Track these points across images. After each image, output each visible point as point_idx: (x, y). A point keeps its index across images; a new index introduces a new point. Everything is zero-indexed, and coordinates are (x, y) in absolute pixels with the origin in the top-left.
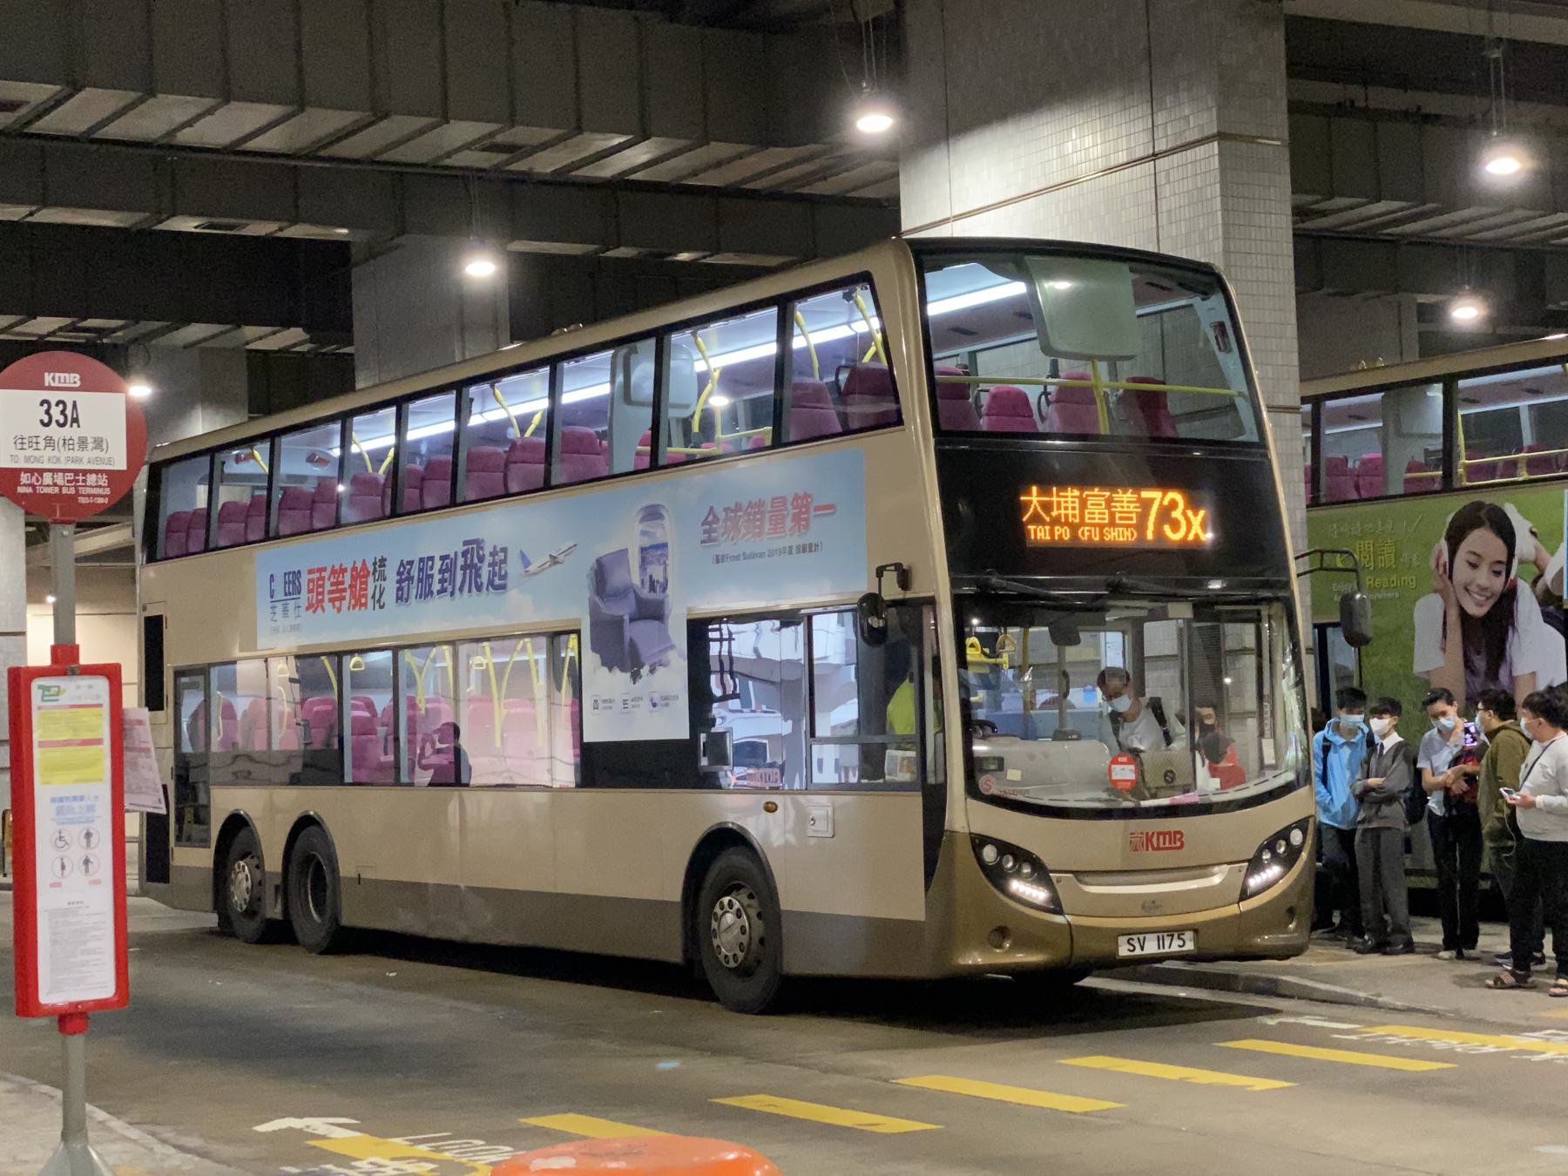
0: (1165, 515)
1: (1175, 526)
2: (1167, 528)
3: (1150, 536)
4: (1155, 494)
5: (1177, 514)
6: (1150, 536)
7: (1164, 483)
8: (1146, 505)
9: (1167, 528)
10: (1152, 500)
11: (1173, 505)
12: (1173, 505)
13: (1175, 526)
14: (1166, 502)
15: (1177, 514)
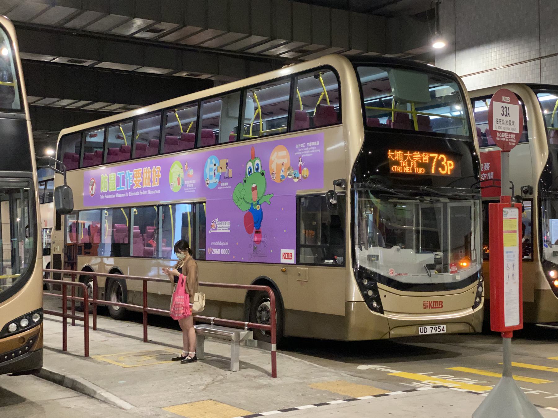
0: (439, 164)
1: (443, 169)
2: (440, 169)
3: (433, 171)
4: (436, 155)
5: (443, 163)
6: (433, 171)
7: (439, 153)
8: (431, 159)
9: (440, 169)
10: (433, 158)
11: (442, 159)
12: (442, 159)
13: (443, 169)
14: (439, 158)
15: (443, 163)
